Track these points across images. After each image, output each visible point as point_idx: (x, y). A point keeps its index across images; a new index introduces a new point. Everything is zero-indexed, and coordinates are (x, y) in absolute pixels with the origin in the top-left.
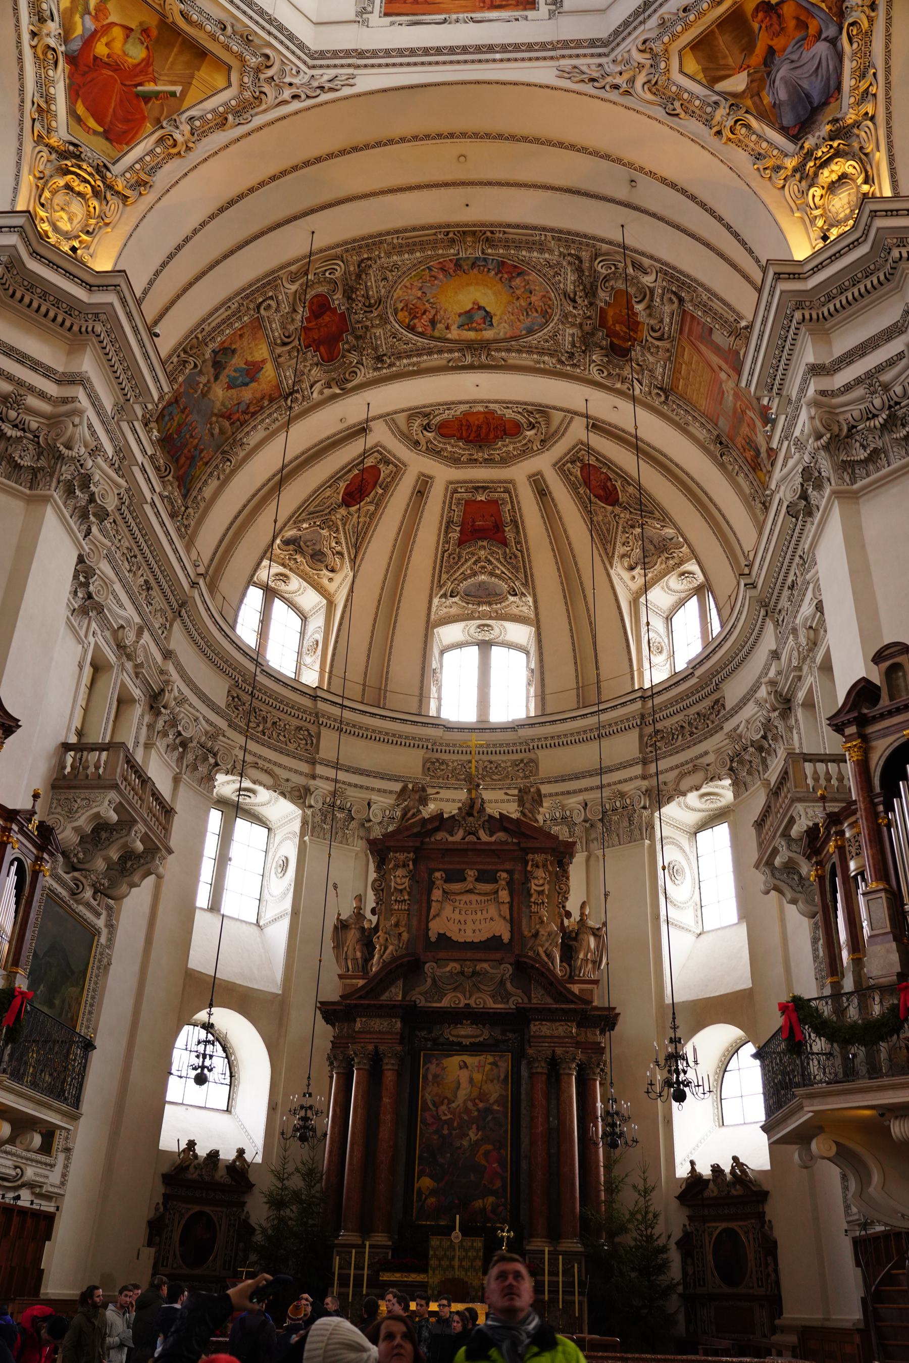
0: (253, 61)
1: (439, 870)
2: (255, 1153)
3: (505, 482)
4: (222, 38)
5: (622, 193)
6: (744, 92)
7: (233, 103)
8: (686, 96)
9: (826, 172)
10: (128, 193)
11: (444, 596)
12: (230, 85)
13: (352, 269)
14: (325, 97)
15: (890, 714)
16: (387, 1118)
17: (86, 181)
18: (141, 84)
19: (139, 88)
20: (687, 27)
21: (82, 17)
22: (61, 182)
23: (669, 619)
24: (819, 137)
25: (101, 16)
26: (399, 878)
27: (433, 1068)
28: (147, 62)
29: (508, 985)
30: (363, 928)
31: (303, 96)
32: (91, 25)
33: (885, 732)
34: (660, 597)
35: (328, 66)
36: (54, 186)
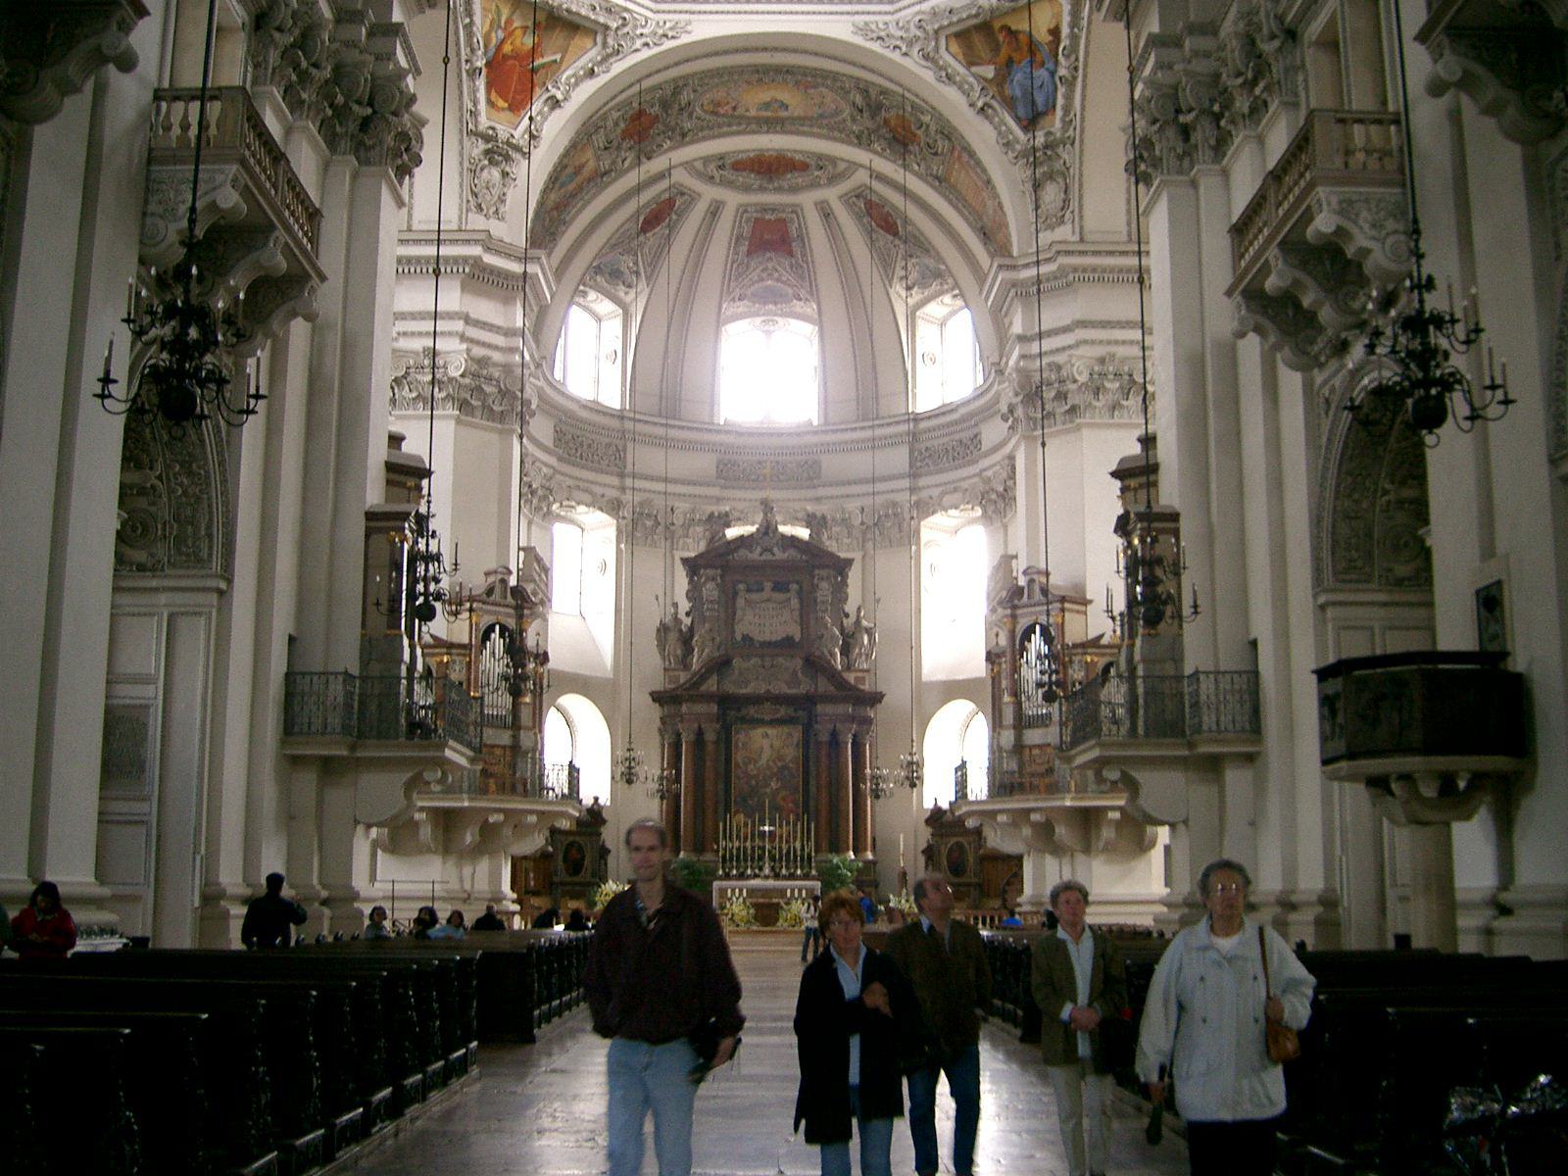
1: (741, 582)
2: (605, 800)
3: (794, 205)
4: (593, 17)
11: (733, 300)
12: (595, 44)
13: (669, 93)
15: (1026, 606)
16: (709, 774)
23: (942, 325)
26: (710, 590)
27: (742, 737)
29: (800, 675)
30: (681, 630)
32: (501, 34)
33: (1024, 615)
34: (935, 309)
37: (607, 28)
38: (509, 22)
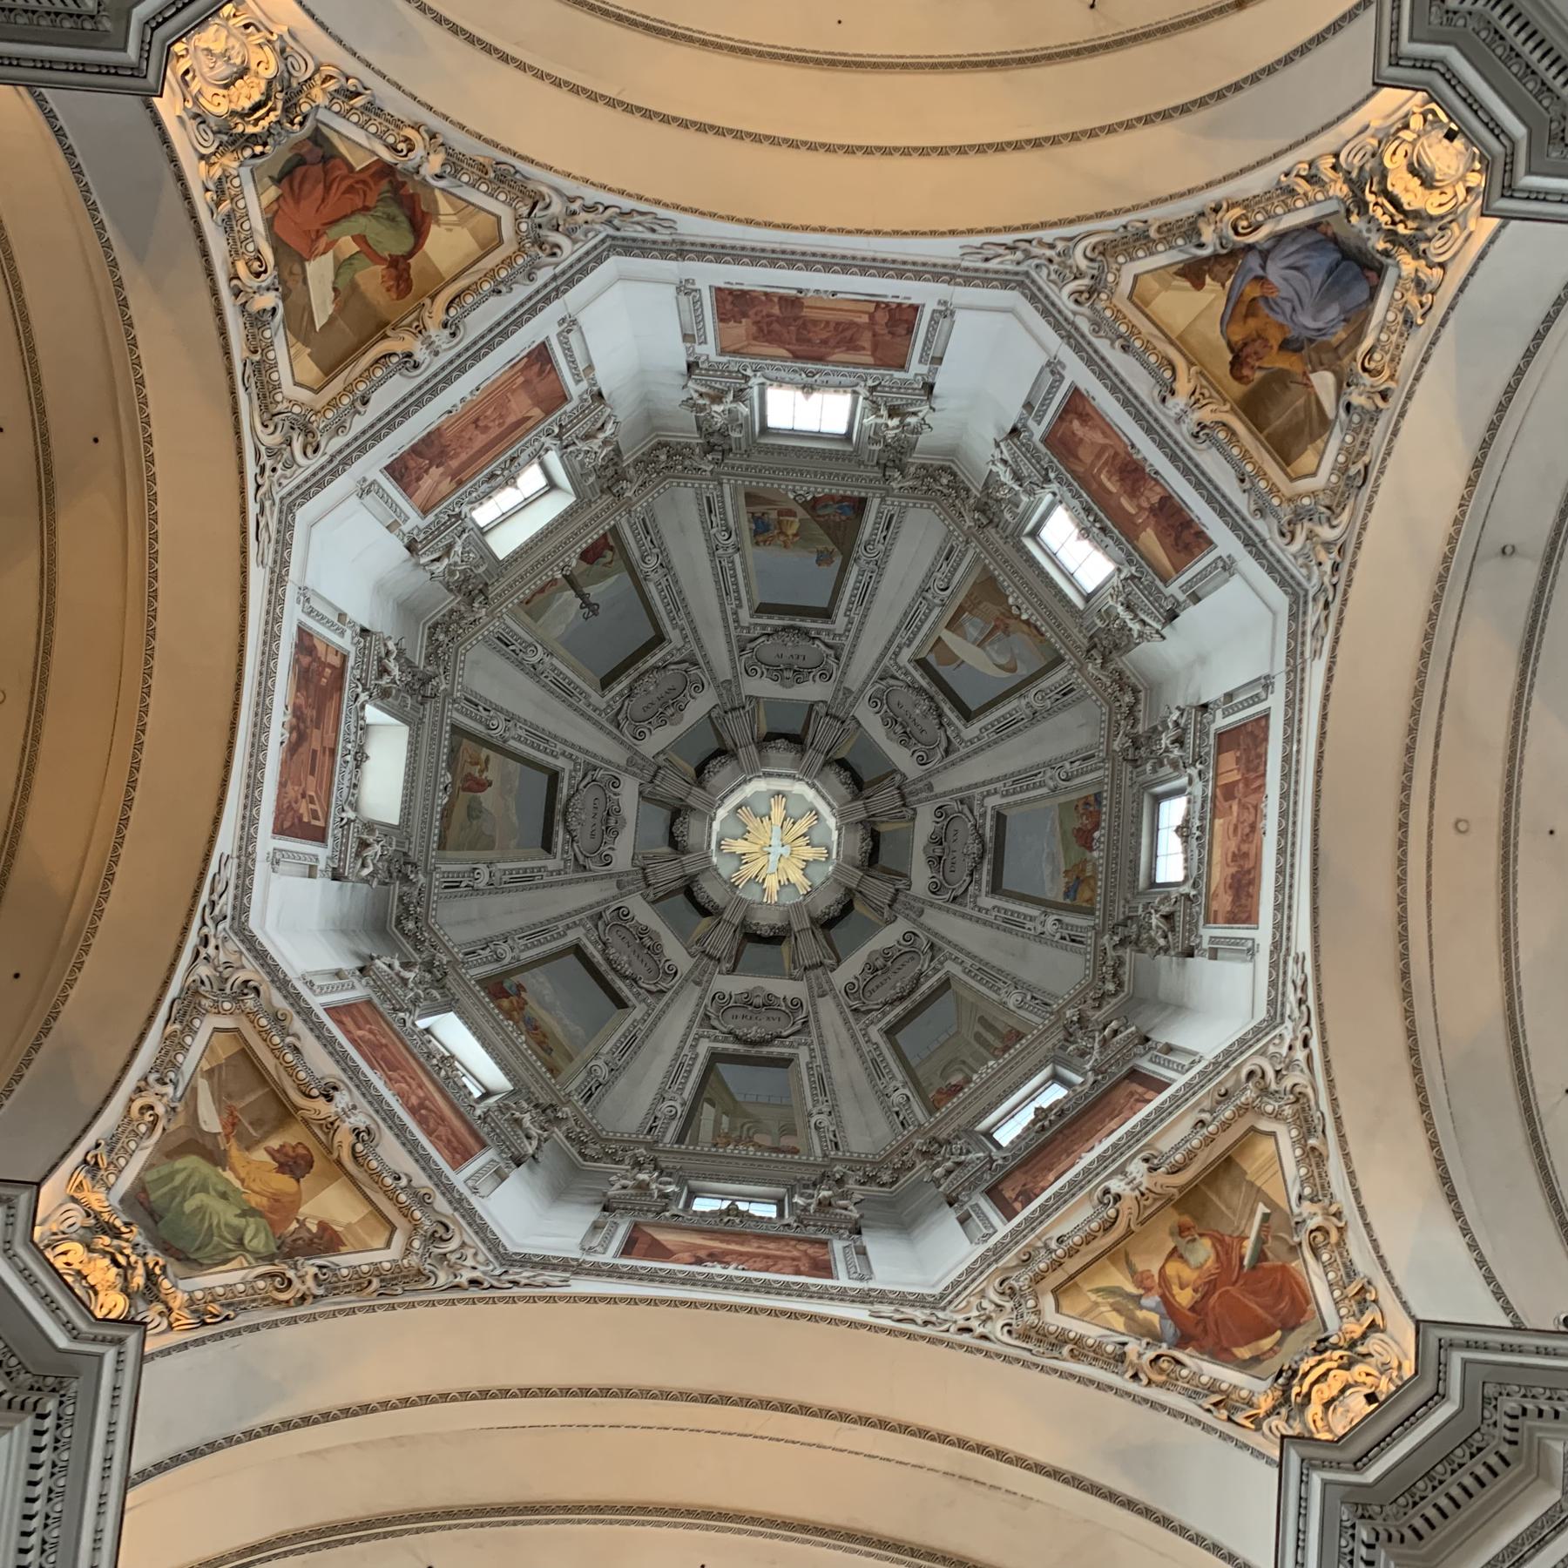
0: (1250, 1094)
4: (1212, 1128)
5: (1527, 571)
6: (1334, 372)
7: (1294, 1133)
8: (1341, 459)
9: (1405, 199)
10: (1366, 1320)
14: (1311, 1002)
17: (1325, 1374)
18: (1242, 1259)
19: (1246, 1262)
20: (1261, 473)
21: (1141, 1308)
22: (1315, 1408)
24: (1369, 230)
25: (1148, 1283)
28: (1219, 1241)
31: (1306, 1031)
32: (1152, 1300)
35: (1284, 994)
36: (1320, 1424)
37: (1244, 1109)
38: (1140, 1279)
